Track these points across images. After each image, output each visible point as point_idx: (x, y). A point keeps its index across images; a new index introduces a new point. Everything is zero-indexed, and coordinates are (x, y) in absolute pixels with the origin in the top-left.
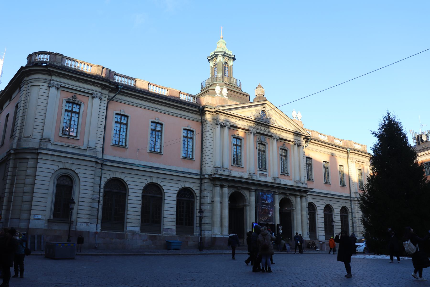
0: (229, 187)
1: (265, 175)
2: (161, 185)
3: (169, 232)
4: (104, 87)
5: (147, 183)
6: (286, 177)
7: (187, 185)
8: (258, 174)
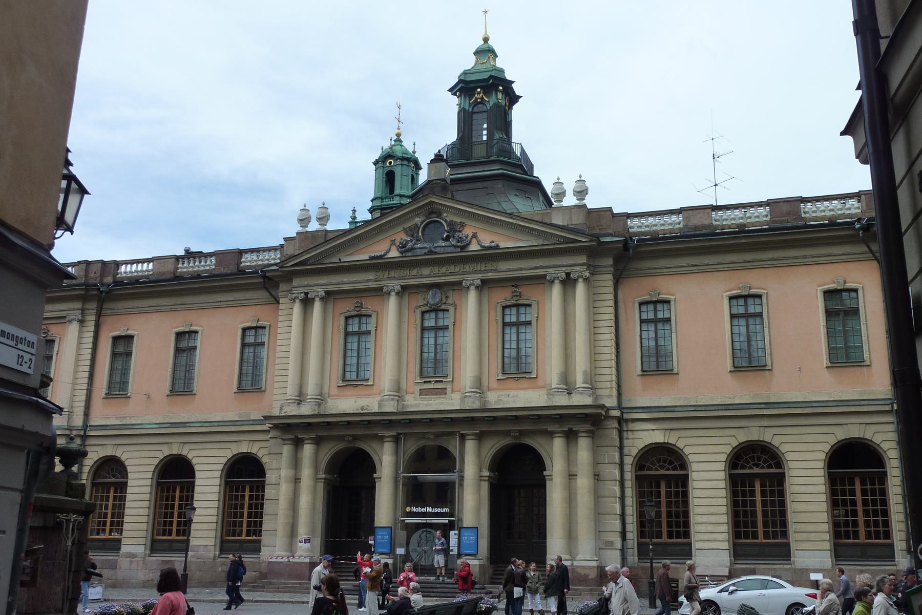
0: (318, 441)
1: (443, 391)
2: (190, 456)
3: (202, 552)
4: (84, 299)
5: (161, 457)
6: (523, 383)
7: (244, 449)
8: (417, 393)
